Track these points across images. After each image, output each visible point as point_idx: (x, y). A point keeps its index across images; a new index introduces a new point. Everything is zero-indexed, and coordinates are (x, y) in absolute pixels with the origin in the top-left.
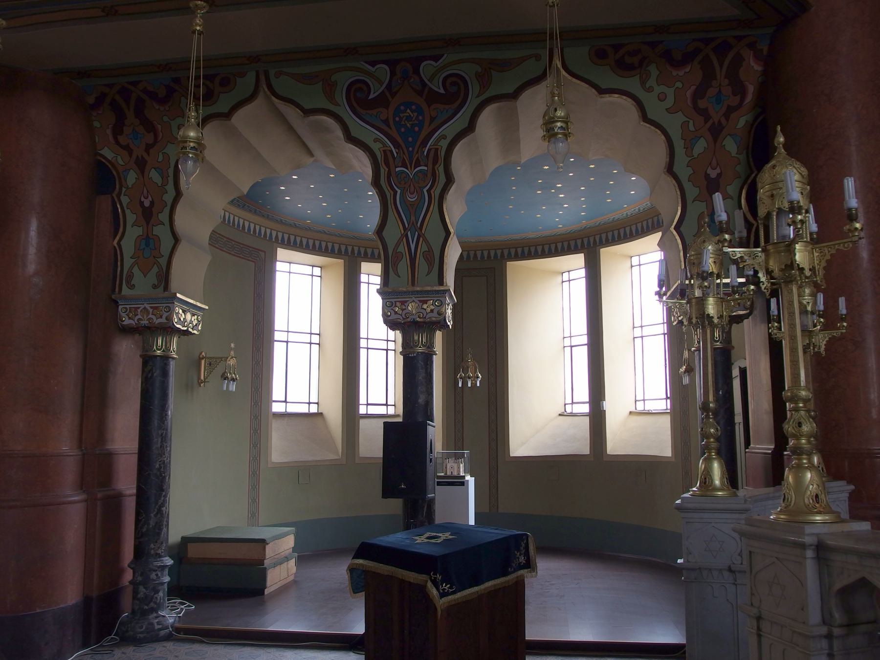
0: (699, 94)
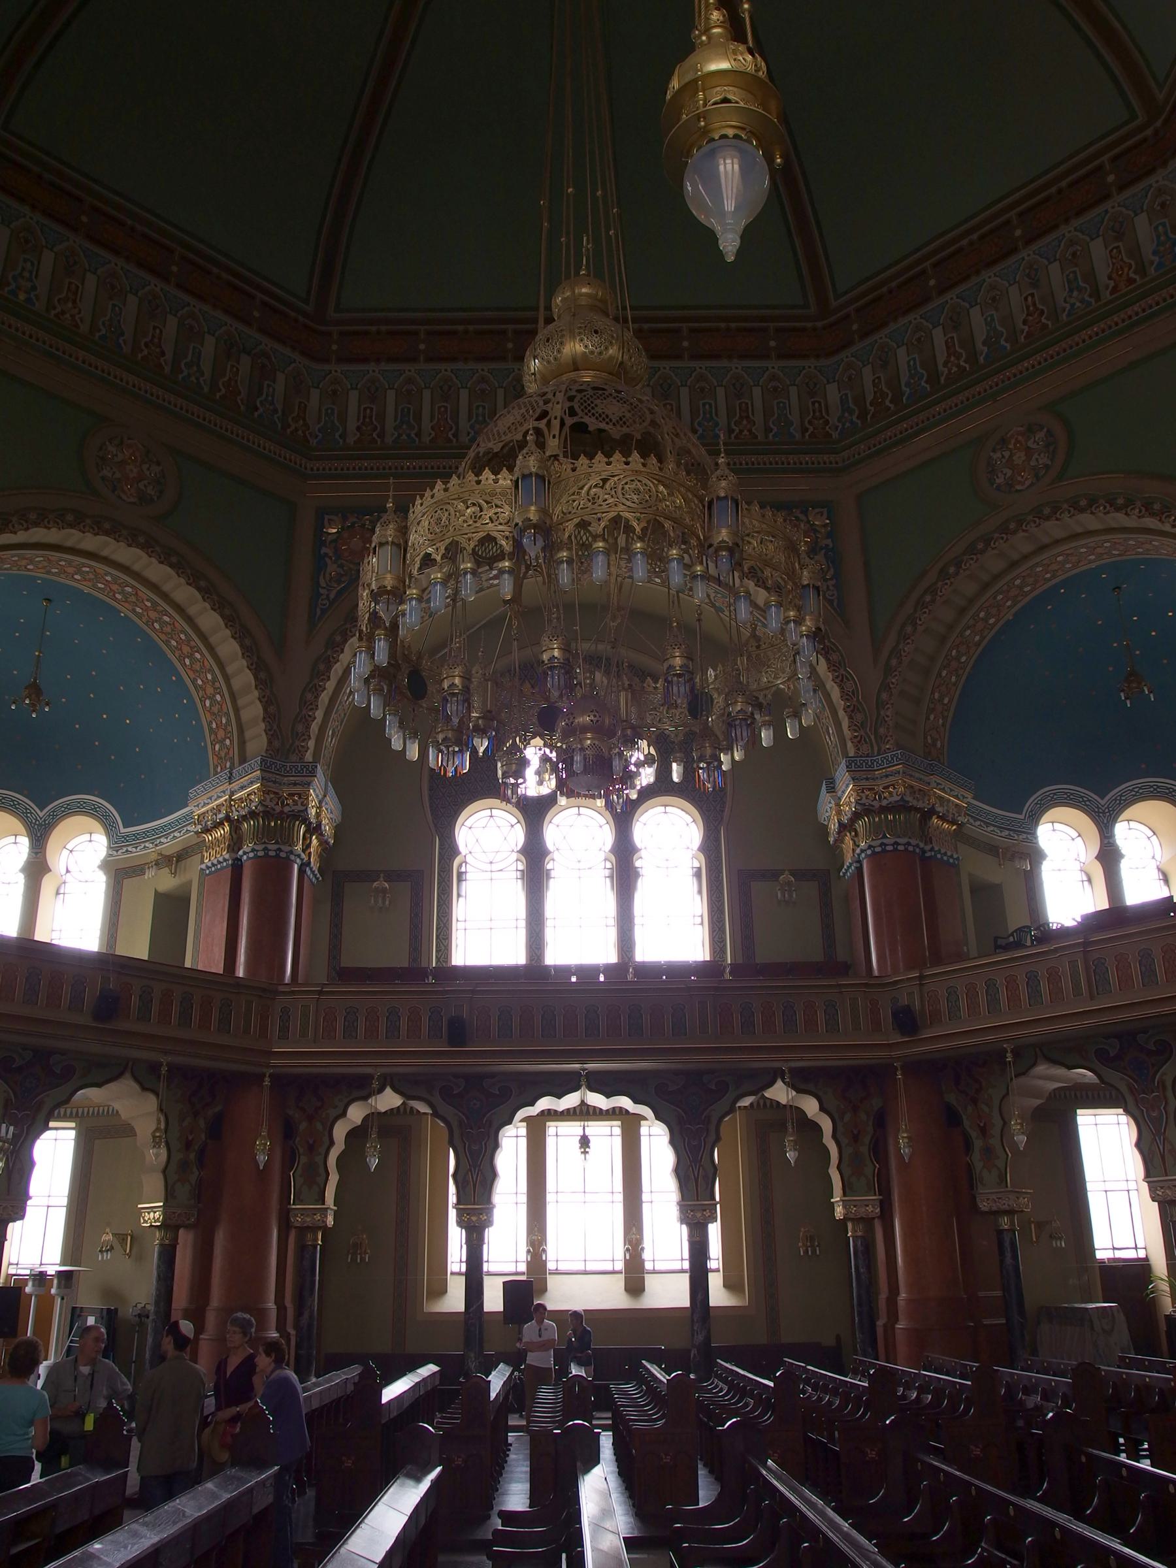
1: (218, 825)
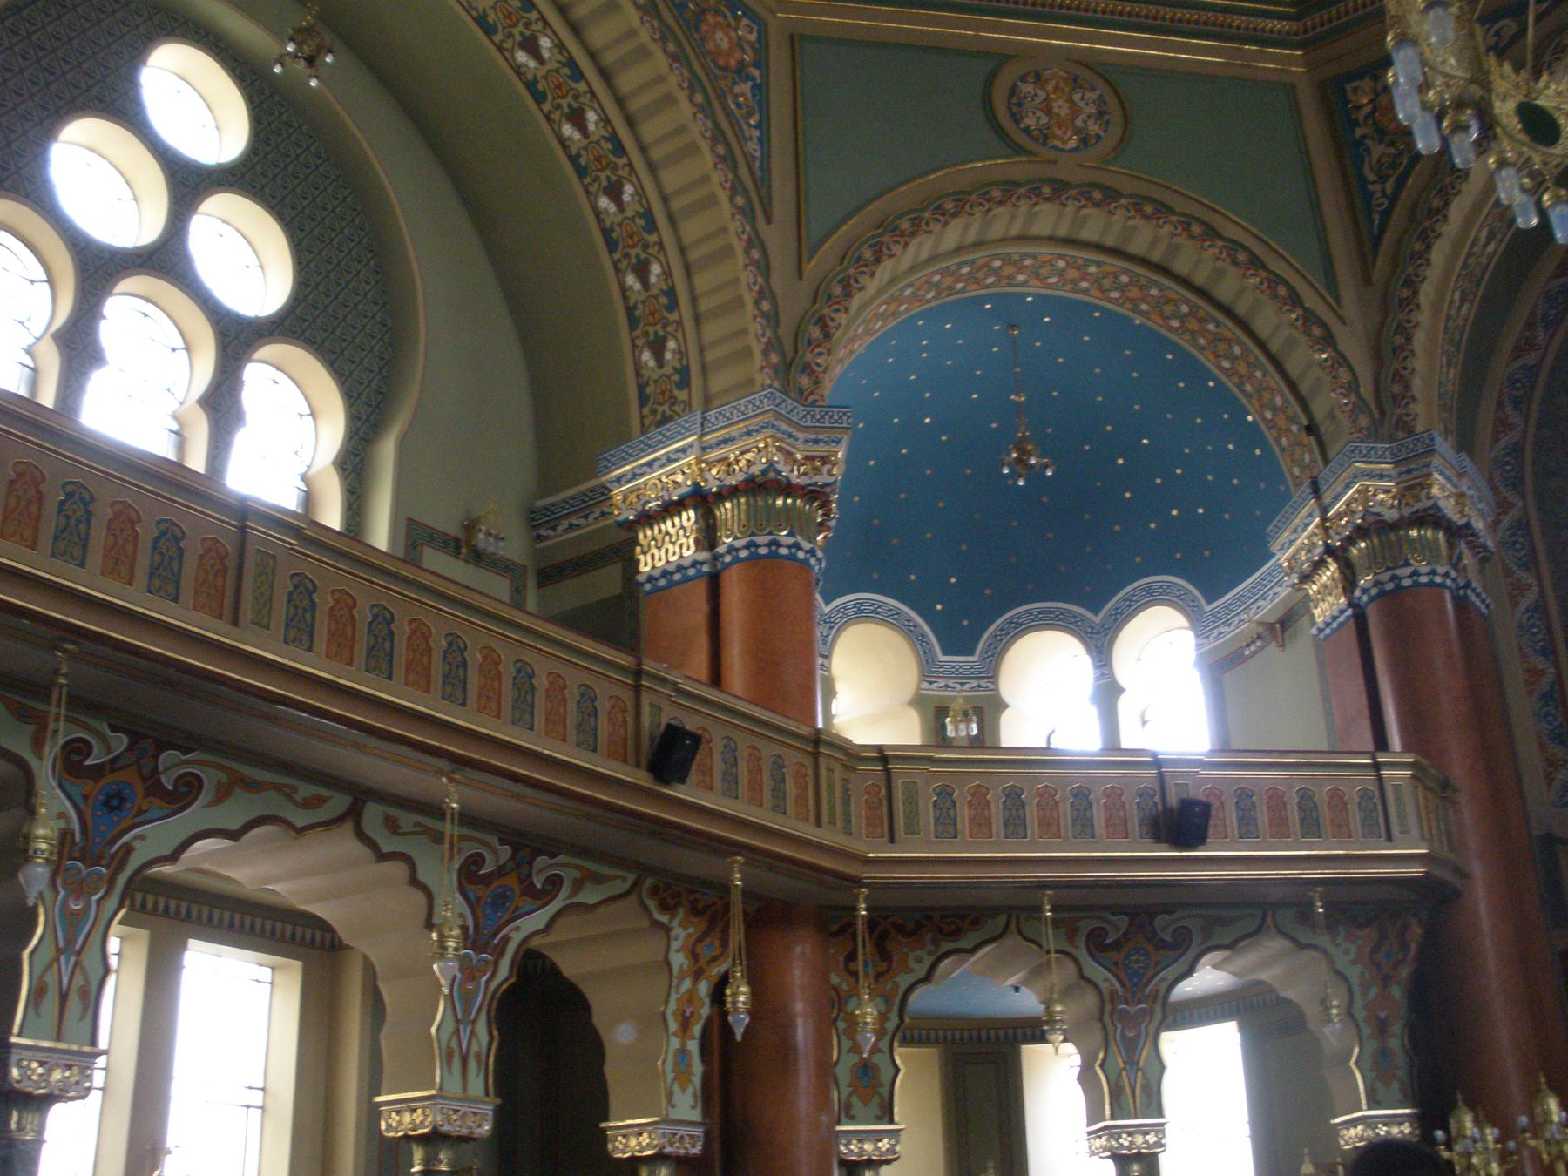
0: (1374, 951)
1: (1319, 565)
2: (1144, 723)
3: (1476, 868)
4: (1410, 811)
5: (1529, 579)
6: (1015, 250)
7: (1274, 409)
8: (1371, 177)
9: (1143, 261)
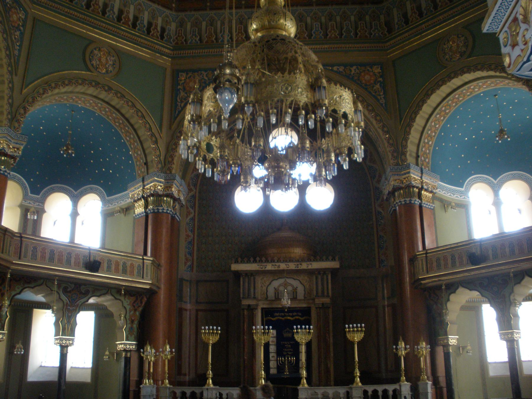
0: (134, 302)
1: (139, 199)
2: (83, 224)
3: (162, 286)
4: (149, 271)
5: (192, 211)
6: (80, 96)
7: (138, 154)
8: (179, 100)
9: (114, 107)
